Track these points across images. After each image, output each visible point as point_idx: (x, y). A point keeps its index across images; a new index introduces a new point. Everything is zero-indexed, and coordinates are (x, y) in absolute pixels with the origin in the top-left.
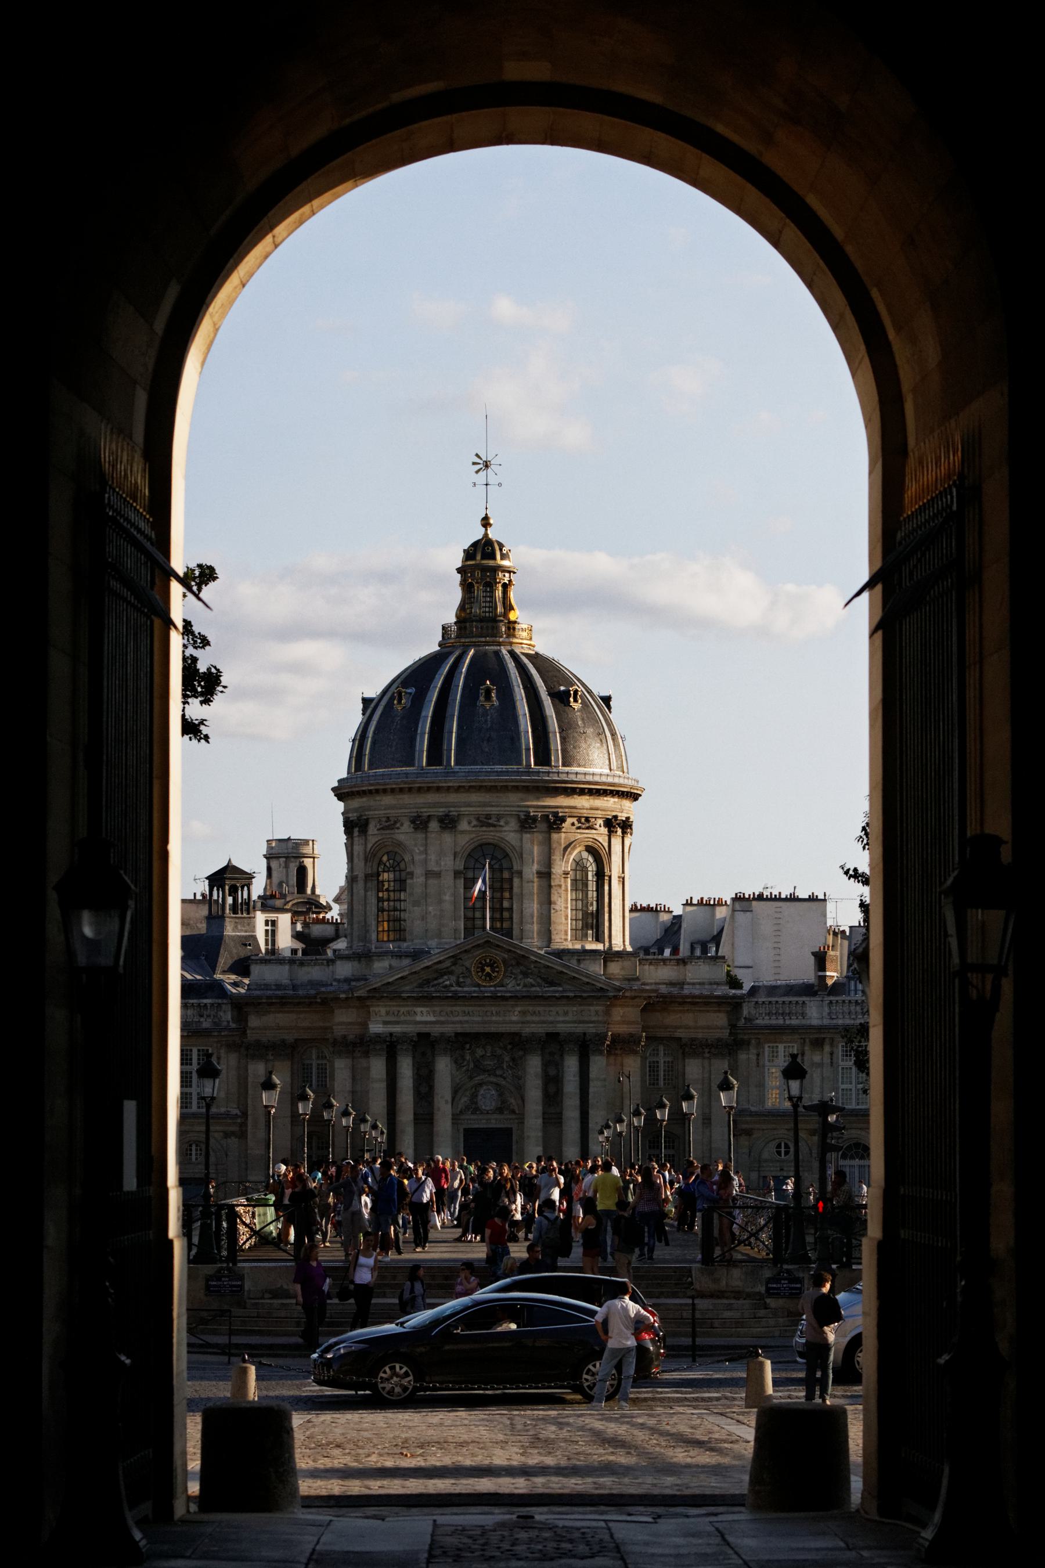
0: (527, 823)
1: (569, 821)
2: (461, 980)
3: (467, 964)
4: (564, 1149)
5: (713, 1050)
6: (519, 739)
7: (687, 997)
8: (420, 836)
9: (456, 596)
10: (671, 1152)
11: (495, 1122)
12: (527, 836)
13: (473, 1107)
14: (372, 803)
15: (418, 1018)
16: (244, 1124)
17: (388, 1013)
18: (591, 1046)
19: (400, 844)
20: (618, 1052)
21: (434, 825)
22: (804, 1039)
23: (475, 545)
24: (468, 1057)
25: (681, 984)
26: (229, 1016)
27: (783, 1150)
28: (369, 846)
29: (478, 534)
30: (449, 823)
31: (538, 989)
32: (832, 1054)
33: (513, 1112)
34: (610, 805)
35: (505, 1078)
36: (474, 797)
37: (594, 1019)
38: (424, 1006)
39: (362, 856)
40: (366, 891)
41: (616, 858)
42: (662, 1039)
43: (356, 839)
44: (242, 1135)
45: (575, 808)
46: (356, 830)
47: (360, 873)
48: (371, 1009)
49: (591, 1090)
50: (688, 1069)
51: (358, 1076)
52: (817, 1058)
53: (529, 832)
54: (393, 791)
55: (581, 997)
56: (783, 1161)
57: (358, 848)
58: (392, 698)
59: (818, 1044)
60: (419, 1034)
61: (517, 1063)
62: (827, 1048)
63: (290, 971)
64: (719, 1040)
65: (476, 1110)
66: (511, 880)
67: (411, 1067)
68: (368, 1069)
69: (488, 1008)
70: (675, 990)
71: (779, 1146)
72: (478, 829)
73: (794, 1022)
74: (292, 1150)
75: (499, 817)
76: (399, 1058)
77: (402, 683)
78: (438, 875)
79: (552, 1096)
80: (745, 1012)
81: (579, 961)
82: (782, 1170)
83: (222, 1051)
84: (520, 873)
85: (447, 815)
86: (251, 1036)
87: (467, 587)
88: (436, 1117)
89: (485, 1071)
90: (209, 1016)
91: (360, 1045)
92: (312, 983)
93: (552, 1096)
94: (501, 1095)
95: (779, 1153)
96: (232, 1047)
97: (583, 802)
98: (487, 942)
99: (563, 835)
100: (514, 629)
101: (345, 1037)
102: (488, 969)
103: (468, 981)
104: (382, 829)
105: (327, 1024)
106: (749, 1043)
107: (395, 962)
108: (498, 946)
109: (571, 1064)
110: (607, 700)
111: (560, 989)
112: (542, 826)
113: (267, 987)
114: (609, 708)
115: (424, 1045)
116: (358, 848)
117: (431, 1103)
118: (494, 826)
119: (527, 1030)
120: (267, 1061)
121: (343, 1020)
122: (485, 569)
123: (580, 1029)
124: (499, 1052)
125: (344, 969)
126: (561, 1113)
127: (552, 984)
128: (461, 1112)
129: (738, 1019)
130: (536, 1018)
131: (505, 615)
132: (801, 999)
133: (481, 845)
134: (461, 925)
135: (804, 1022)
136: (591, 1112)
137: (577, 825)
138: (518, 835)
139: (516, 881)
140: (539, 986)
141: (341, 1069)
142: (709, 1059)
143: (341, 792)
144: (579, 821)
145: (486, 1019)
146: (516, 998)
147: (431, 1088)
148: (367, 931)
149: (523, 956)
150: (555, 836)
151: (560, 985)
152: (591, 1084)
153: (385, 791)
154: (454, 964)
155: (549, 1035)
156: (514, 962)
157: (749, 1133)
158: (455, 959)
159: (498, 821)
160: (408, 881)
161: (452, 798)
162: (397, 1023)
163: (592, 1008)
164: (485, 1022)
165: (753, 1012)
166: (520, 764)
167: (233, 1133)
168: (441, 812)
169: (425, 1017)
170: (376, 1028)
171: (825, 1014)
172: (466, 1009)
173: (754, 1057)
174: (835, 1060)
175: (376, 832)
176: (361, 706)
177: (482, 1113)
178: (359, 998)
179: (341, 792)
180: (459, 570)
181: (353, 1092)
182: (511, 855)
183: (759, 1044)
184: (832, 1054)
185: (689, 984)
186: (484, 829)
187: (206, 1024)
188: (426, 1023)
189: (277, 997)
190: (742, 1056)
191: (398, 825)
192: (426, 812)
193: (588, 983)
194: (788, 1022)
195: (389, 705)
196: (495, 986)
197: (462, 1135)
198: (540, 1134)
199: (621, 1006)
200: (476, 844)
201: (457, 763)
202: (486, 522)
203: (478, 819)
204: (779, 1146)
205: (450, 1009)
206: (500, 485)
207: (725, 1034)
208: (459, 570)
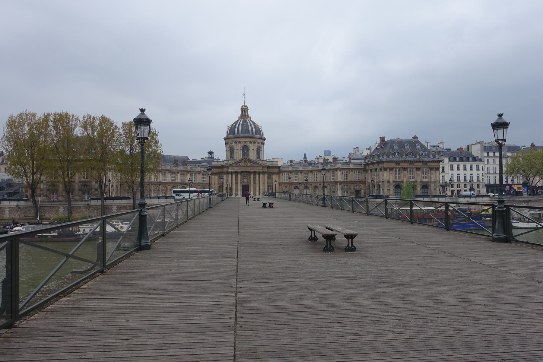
0: (251, 142)
9: (241, 113)
11: (246, 184)
30: (240, 142)
34: (262, 140)
51: (227, 177)
59: (291, 173)
61: (250, 175)
79: (255, 180)
87: (242, 111)
91: (228, 173)
93: (255, 180)
97: (258, 140)
109: (257, 176)
115: (236, 173)
121: (225, 170)
125: (225, 162)
141: (225, 176)
143: (225, 139)
146: (250, 166)
169: (236, 169)
170: (229, 170)
179: (225, 139)
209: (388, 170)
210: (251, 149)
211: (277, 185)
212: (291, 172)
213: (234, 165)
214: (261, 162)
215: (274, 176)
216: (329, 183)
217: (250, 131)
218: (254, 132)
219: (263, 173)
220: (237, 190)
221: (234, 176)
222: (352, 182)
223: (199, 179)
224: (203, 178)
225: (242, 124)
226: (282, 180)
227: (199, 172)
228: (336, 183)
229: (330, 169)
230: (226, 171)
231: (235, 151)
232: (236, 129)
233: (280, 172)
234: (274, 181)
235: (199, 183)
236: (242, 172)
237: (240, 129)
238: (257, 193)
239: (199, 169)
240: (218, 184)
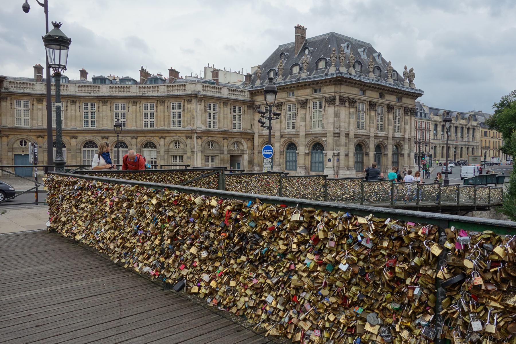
27: (23, 143)
52: (40, 106)
56: (24, 148)
71: (21, 142)
95: (22, 145)
106: (6, 99)
157: (7, 136)
165: (8, 85)
183: (11, 99)
194: (26, 91)
204: (21, 142)
209: (347, 104)
216: (163, 134)
222: (226, 135)
228: (190, 134)
229: (168, 97)
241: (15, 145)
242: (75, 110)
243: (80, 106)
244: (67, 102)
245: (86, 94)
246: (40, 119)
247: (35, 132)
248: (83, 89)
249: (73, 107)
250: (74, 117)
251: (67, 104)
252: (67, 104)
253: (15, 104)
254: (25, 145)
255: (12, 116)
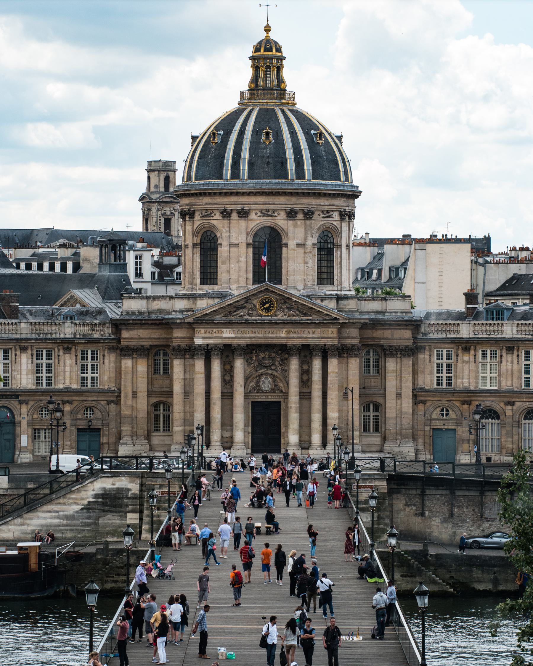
0: (291, 214)
1: (316, 213)
2: (250, 312)
3: (255, 302)
4: (313, 415)
5: (403, 352)
6: (286, 163)
7: (387, 321)
8: (226, 221)
9: (249, 74)
10: (377, 413)
12: (291, 222)
13: (258, 388)
14: (198, 201)
15: (224, 335)
16: (119, 396)
17: (205, 332)
18: (329, 352)
19: (214, 226)
20: (345, 355)
21: (234, 215)
22: (458, 346)
23: (260, 43)
24: (254, 358)
25: (383, 313)
26: (110, 332)
27: (445, 413)
28: (195, 227)
29: (263, 35)
30: (244, 214)
31: (297, 318)
32: (475, 356)
33: (282, 391)
35: (277, 371)
36: (259, 199)
37: (332, 336)
38: (228, 328)
39: (191, 234)
40: (193, 254)
41: (344, 235)
42: (372, 345)
43: (187, 222)
44: (118, 402)
45: (320, 205)
46: (187, 216)
47: (190, 245)
48: (196, 329)
49: (329, 379)
50: (388, 365)
51: (188, 370)
52: (466, 358)
53: (292, 220)
54: (210, 194)
55: (323, 323)
57: (189, 228)
58: (209, 137)
59: (466, 350)
60: (225, 345)
61: (285, 362)
62: (472, 352)
63: (147, 304)
64: (407, 347)
65: (260, 390)
66: (282, 248)
67: (219, 363)
68: (194, 365)
69: (267, 329)
70: (380, 317)
71: (442, 410)
72: (261, 218)
73: (453, 336)
74: (148, 412)
75: (274, 211)
76: (212, 360)
77: (216, 127)
78: (237, 245)
79: (305, 382)
80: (422, 330)
81: (322, 301)
82: (444, 425)
83: (106, 352)
84: (286, 245)
85: (242, 209)
86: (123, 343)
87: (256, 69)
88: (234, 395)
89: (265, 367)
90: (97, 331)
91: (189, 351)
92: (161, 311)
93: (305, 382)
94: (274, 381)
95: (443, 415)
96: (112, 349)
97: (325, 202)
98: (267, 289)
99: (313, 222)
100: (284, 94)
101: (179, 346)
102: (267, 306)
103: (255, 313)
104: (203, 217)
105: (169, 336)
106: (424, 348)
107: (211, 302)
108: (273, 291)
109: (317, 364)
110: (340, 138)
111: (311, 318)
112: (300, 216)
113: (133, 313)
114: (341, 143)
115: (228, 352)
116: (189, 228)
117: (232, 386)
118: (271, 216)
119: (290, 342)
120: (133, 358)
121: (178, 334)
122: (266, 58)
123: (322, 342)
124: (273, 355)
125: (180, 304)
126: (311, 392)
127: (305, 315)
128: (250, 391)
129: (418, 334)
130: (295, 335)
131: (279, 85)
132: (456, 322)
133: (263, 228)
134: (251, 276)
135: (458, 336)
136: (329, 392)
137: (322, 215)
138: (286, 222)
139: (284, 250)
140: (298, 316)
141: (178, 367)
142: (401, 358)
144: (323, 212)
145: (267, 335)
146: (284, 324)
147: (232, 377)
148: (194, 278)
149: (288, 298)
150: (308, 222)
151: (310, 315)
152: (329, 376)
153: (205, 194)
154: (246, 302)
155: (303, 345)
156: (282, 301)
157: (424, 402)
158: (247, 299)
159: (274, 213)
160: (219, 249)
161: (245, 199)
162: (211, 338)
163: (330, 329)
164: (265, 338)
166: (287, 178)
167: (112, 401)
168: (239, 207)
171: (471, 331)
172: (253, 330)
173: (427, 357)
174: (477, 359)
175: (199, 219)
176: (191, 140)
177: (263, 392)
178: (188, 323)
180: (251, 58)
181: (185, 379)
182: (281, 234)
183: (430, 350)
184: (475, 356)
185: (388, 312)
186: (265, 218)
187: (96, 335)
188: (229, 338)
189: (139, 320)
190: (421, 356)
191: (213, 215)
192: (229, 207)
193: (327, 315)
194: (448, 336)
195: (207, 142)
196: (271, 316)
197: (250, 406)
198: (298, 406)
199: (347, 327)
200: (260, 227)
201: (249, 178)
202: (268, 29)
203: (261, 212)
204: (442, 410)
205: (243, 329)
206: (276, 6)
207: (410, 343)
208: (251, 58)
210: (292, 244)
211: (407, 403)
212: (466, 346)
213: (218, 317)
214: (331, 304)
215: (391, 364)
217: (291, 164)
218: (307, 165)
219: (343, 351)
220: (228, 423)
221: (216, 366)
223: (67, 373)
224: (84, 369)
225: (256, 133)
226: (428, 381)
227: (67, 345)
230: (184, 343)
231: (223, 251)
232: (229, 154)
233: (411, 351)
234: (391, 384)
235: (68, 391)
236: (250, 350)
237: (245, 154)
238: (316, 438)
239: (68, 330)
240: (150, 393)
241: (434, 416)
242: (512, 362)
243: (518, 356)
244: (501, 350)
245: (527, 336)
246: (466, 377)
247: (460, 396)
248: (523, 328)
249: (510, 357)
250: (510, 372)
251: (501, 353)
252: (501, 353)
253: (435, 355)
254: (447, 415)
255: (431, 373)
